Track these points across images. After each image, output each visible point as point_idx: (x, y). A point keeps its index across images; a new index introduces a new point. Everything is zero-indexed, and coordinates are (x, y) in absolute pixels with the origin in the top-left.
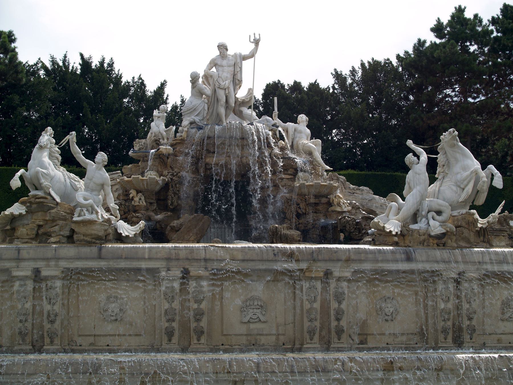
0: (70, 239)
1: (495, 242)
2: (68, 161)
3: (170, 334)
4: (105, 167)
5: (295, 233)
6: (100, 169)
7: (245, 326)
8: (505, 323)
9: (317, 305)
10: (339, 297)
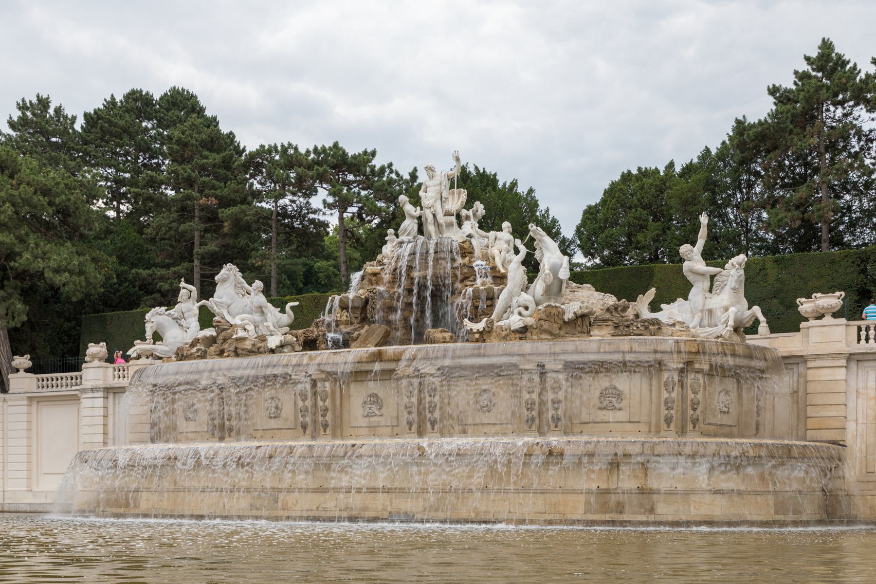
0: (237, 355)
3: (304, 427)
4: (263, 292)
6: (256, 295)
7: (367, 420)
8: (605, 412)
9: (414, 400)
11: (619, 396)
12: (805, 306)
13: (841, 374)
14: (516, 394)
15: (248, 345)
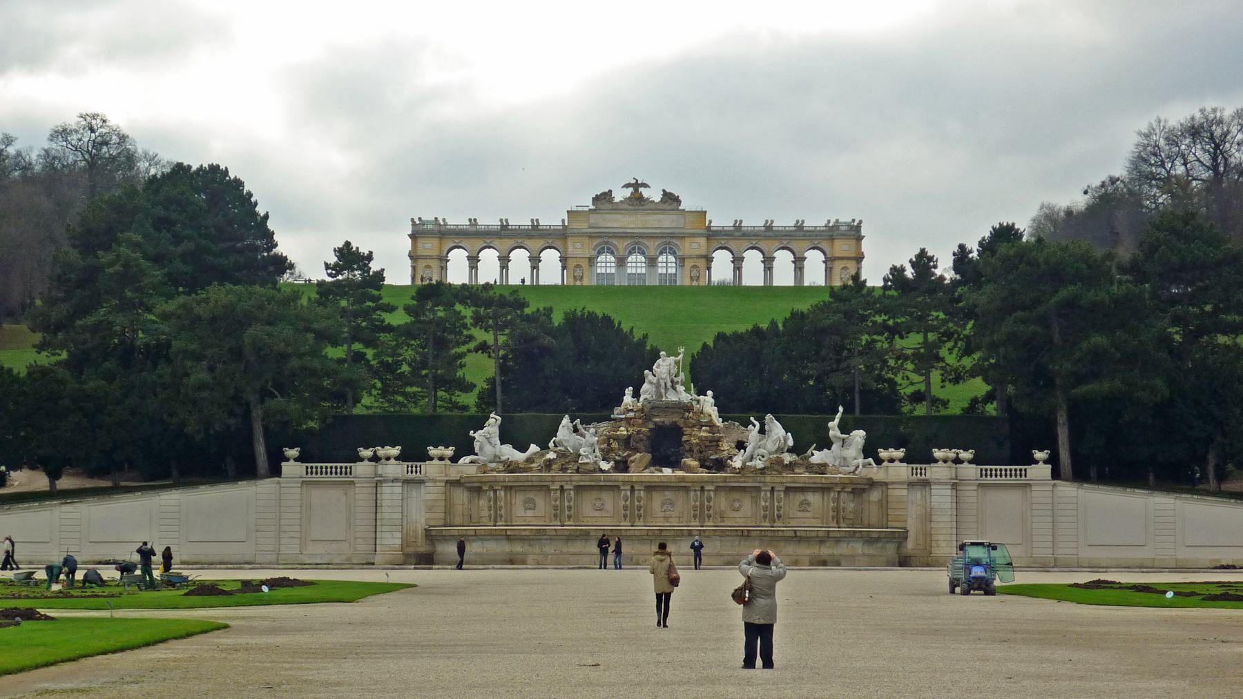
0: (578, 471)
1: (797, 470)
2: (576, 430)
3: (625, 516)
5: (695, 463)
10: (709, 500)
11: (809, 504)
12: (883, 454)
13: (905, 492)
14: (755, 501)
15: (591, 467)
